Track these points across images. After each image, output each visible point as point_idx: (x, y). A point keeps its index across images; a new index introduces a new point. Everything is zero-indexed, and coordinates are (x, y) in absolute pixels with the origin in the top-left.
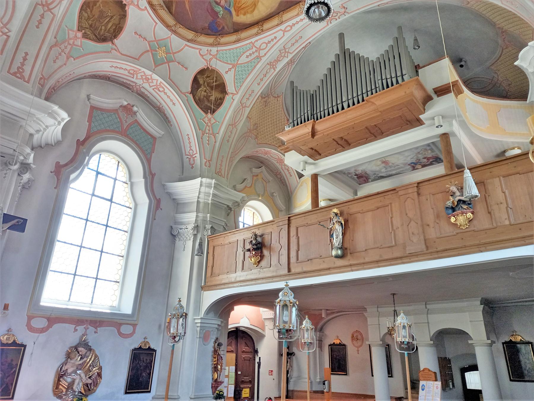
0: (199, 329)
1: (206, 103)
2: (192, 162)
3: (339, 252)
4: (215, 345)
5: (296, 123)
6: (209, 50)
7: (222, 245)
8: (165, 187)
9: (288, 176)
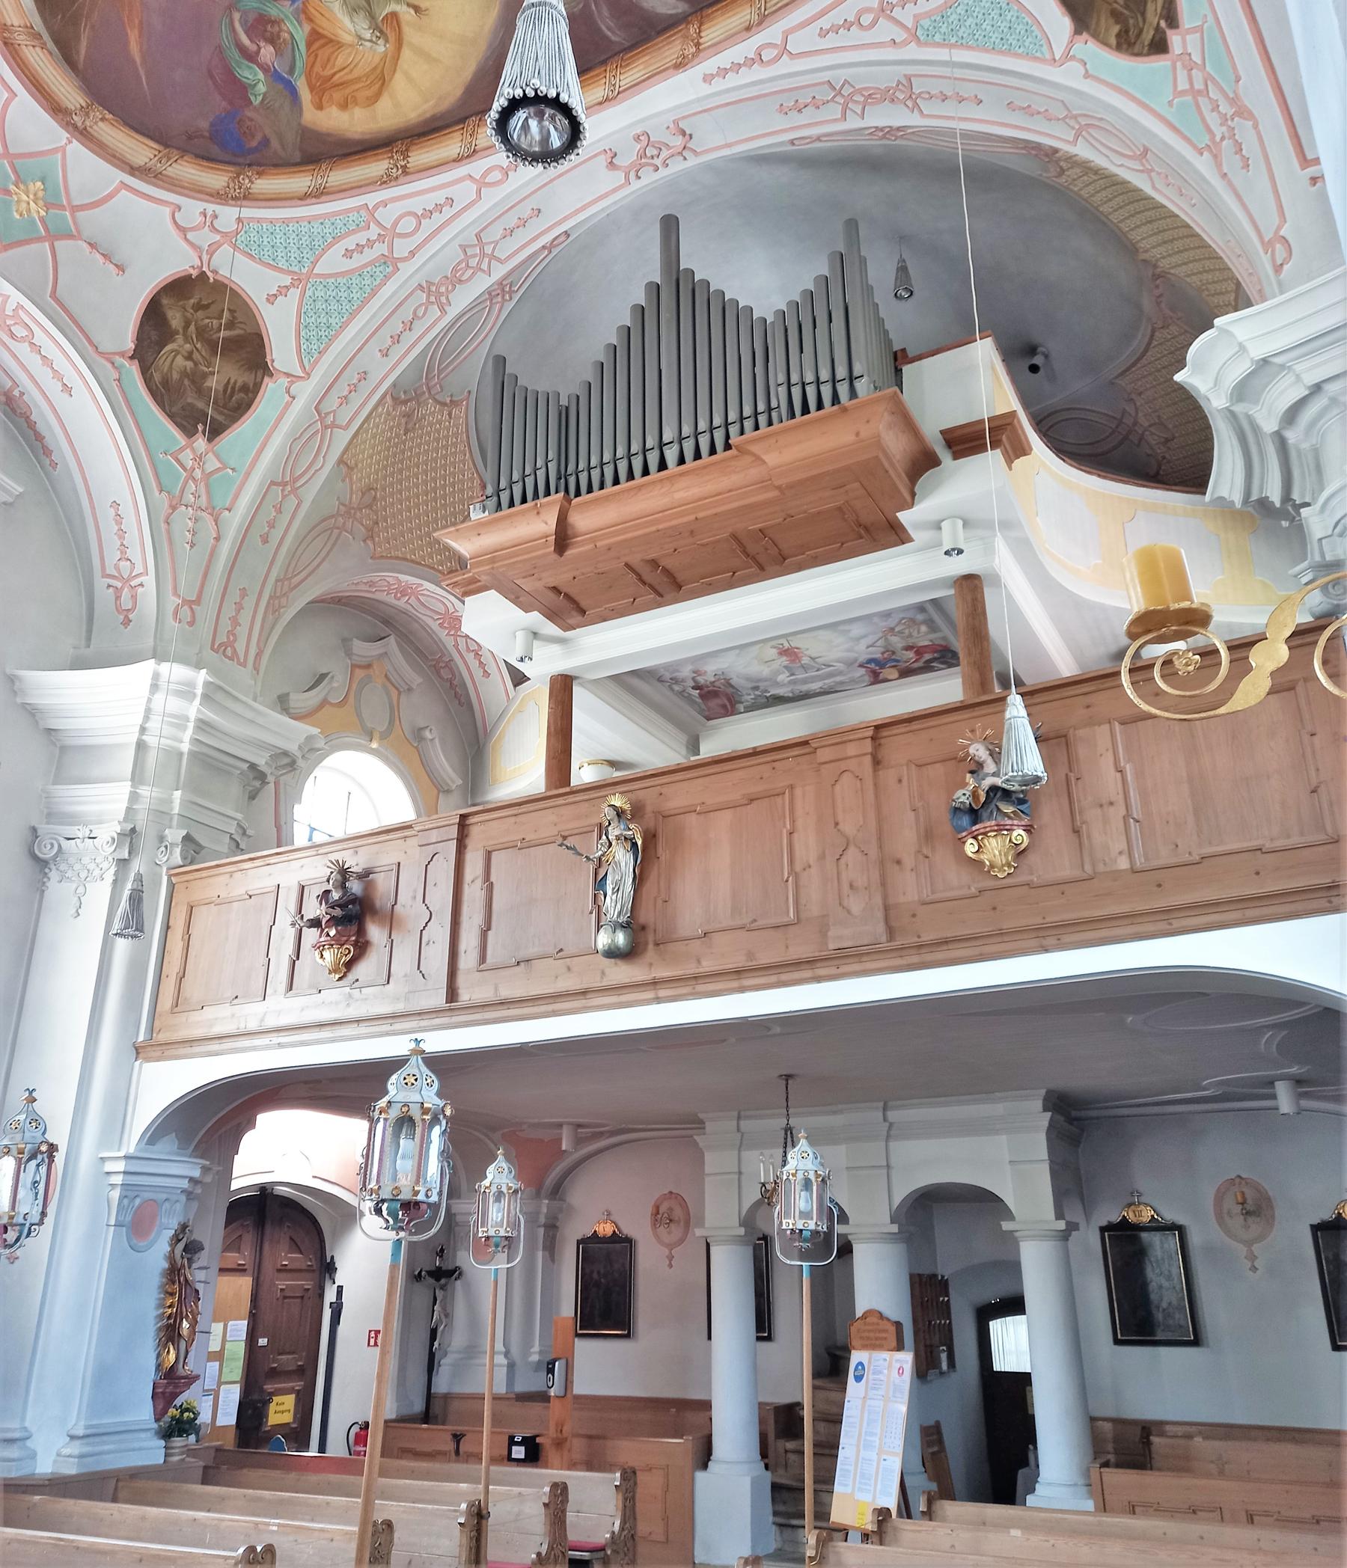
0: (116, 1194)
1: (191, 398)
2: (126, 602)
3: (621, 938)
4: (173, 1251)
5: (505, 497)
6: (209, 213)
7: (220, 902)
8: (17, 683)
9: (478, 673)
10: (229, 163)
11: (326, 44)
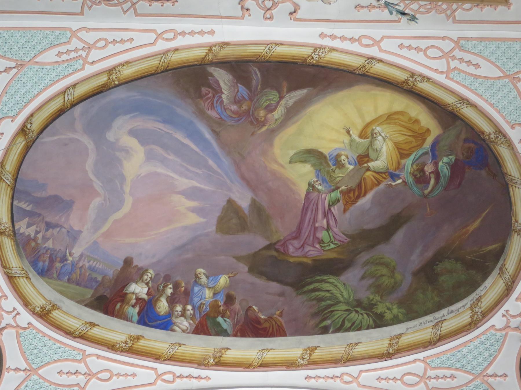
10: (491, 150)
11: (401, 149)
